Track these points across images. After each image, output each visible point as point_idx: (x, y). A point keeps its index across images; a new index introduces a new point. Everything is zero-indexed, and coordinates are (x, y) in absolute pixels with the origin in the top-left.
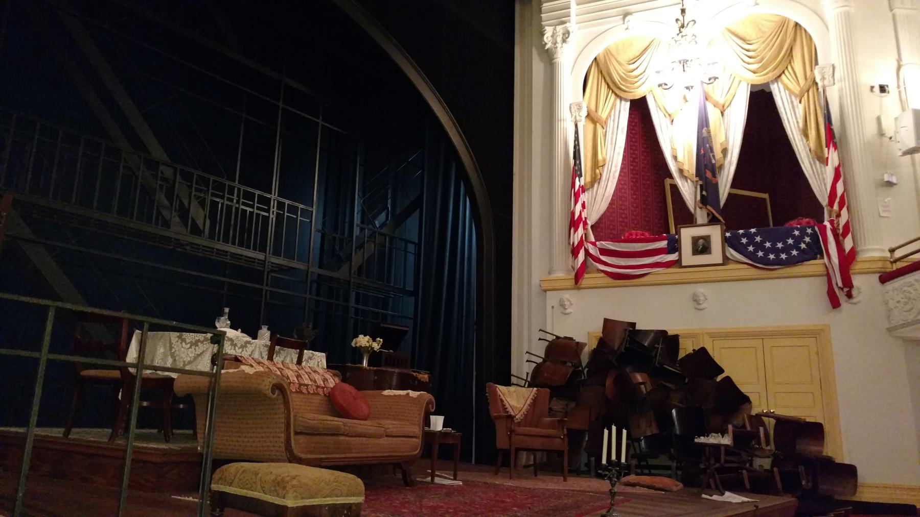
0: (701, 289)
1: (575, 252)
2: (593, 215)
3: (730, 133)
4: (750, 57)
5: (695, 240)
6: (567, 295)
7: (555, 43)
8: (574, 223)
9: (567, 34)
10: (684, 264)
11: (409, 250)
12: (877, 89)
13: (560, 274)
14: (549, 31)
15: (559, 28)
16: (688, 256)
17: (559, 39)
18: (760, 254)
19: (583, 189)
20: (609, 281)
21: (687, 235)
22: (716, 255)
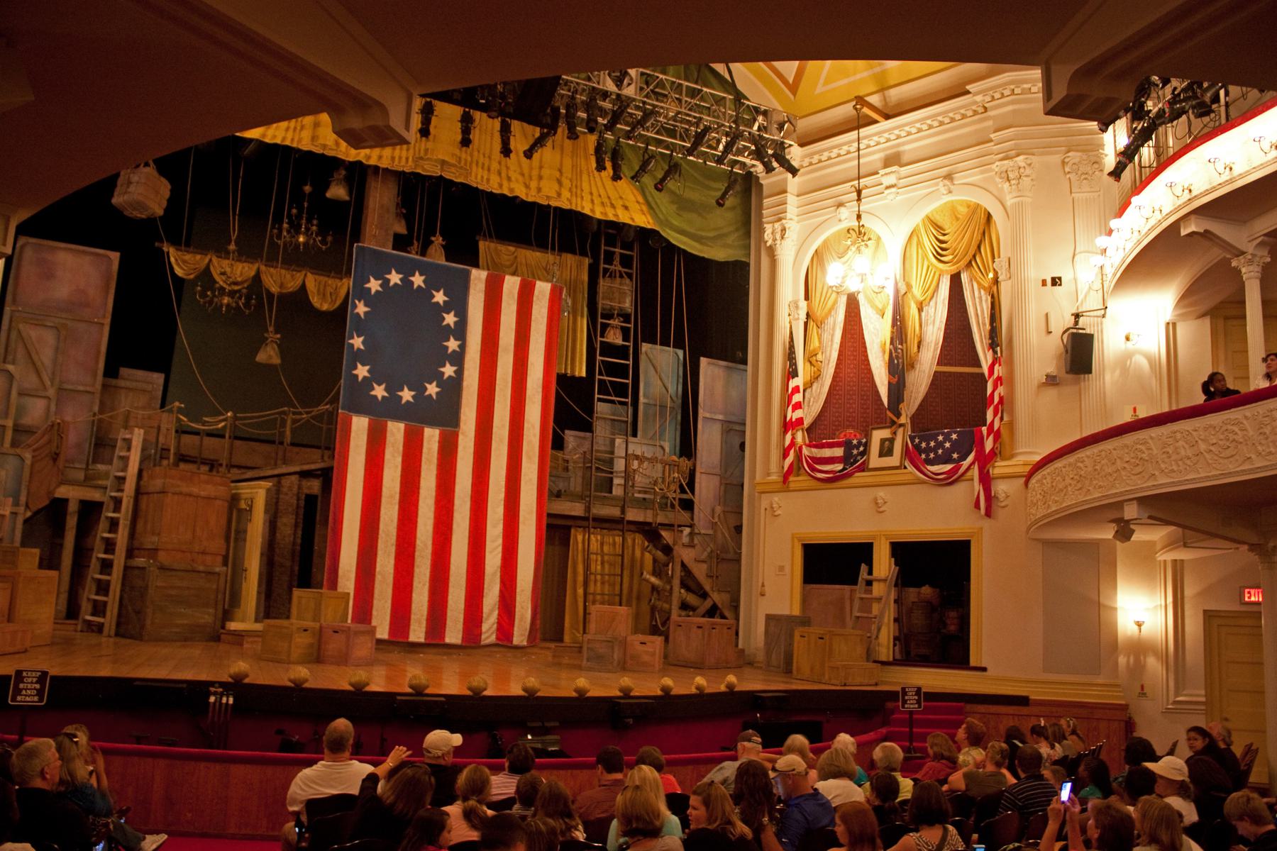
0: (881, 493)
1: (785, 455)
2: (808, 414)
3: (932, 325)
4: (943, 249)
5: (883, 441)
6: (776, 498)
7: (775, 240)
8: (787, 426)
9: (784, 230)
10: (871, 465)
11: (623, 461)
12: (1049, 282)
13: (774, 478)
14: (768, 229)
15: (777, 225)
16: (875, 460)
17: (778, 236)
18: (932, 455)
19: (796, 389)
20: (814, 483)
21: (878, 435)
22: (894, 460)
